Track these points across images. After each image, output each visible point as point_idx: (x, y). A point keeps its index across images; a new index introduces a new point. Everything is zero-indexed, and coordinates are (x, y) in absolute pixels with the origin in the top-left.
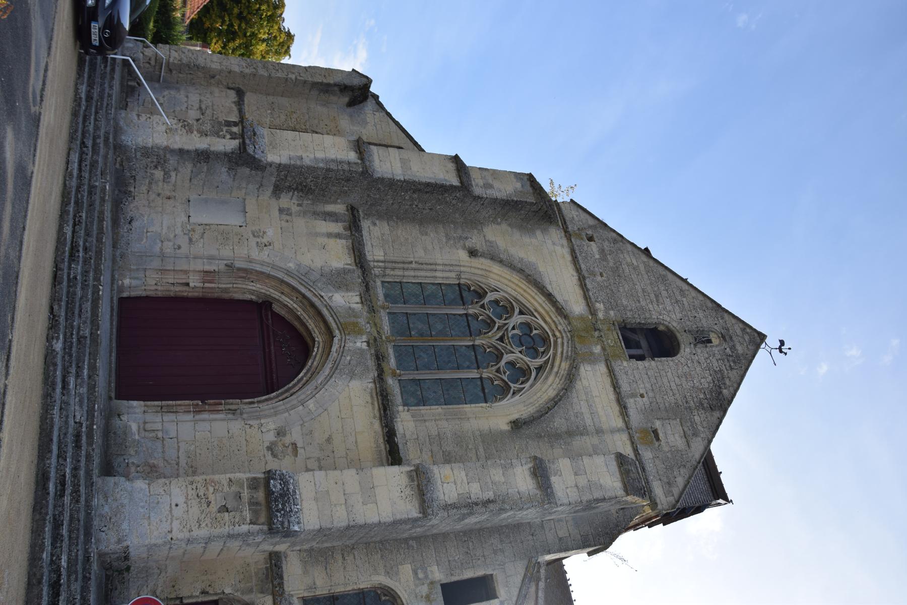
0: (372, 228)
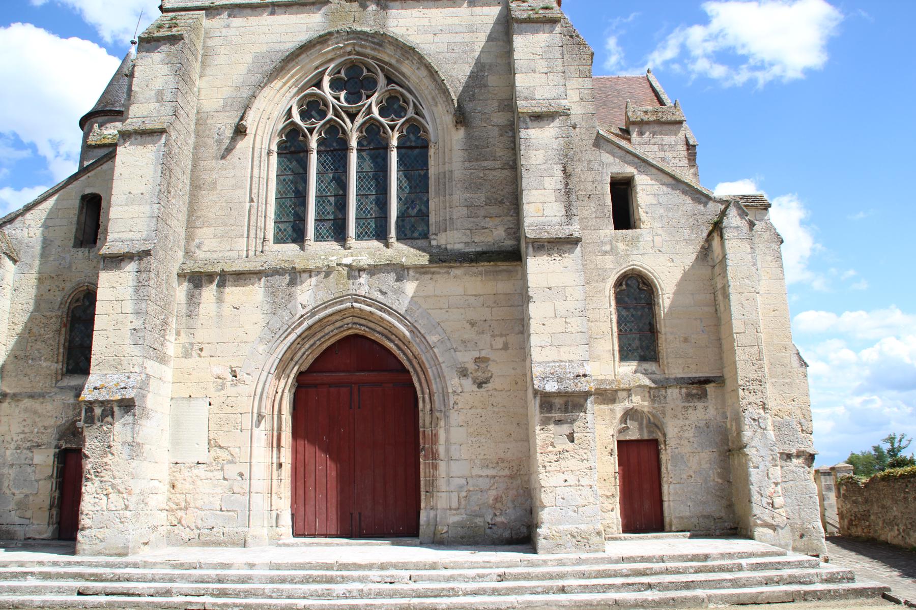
0: (205, 248)
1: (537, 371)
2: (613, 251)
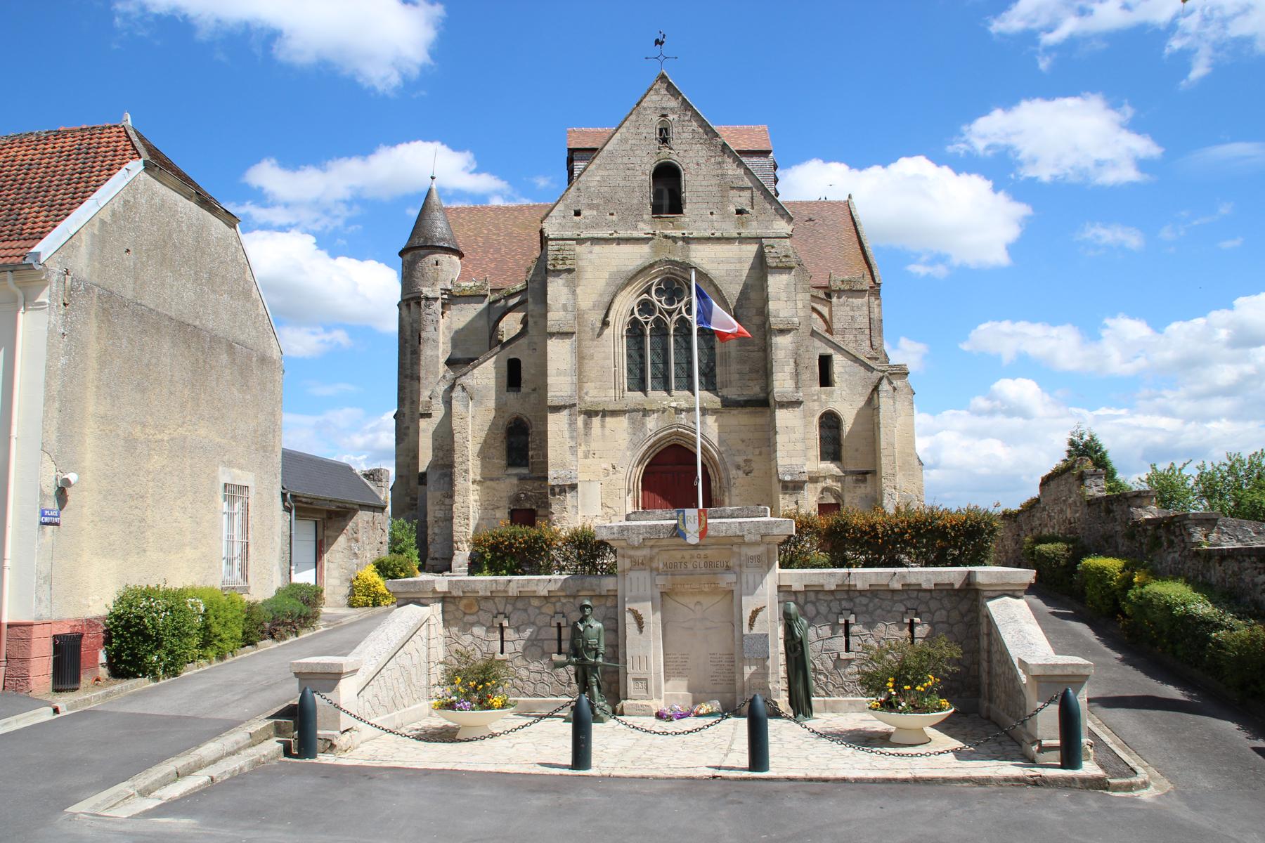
1: (780, 470)
2: (819, 400)
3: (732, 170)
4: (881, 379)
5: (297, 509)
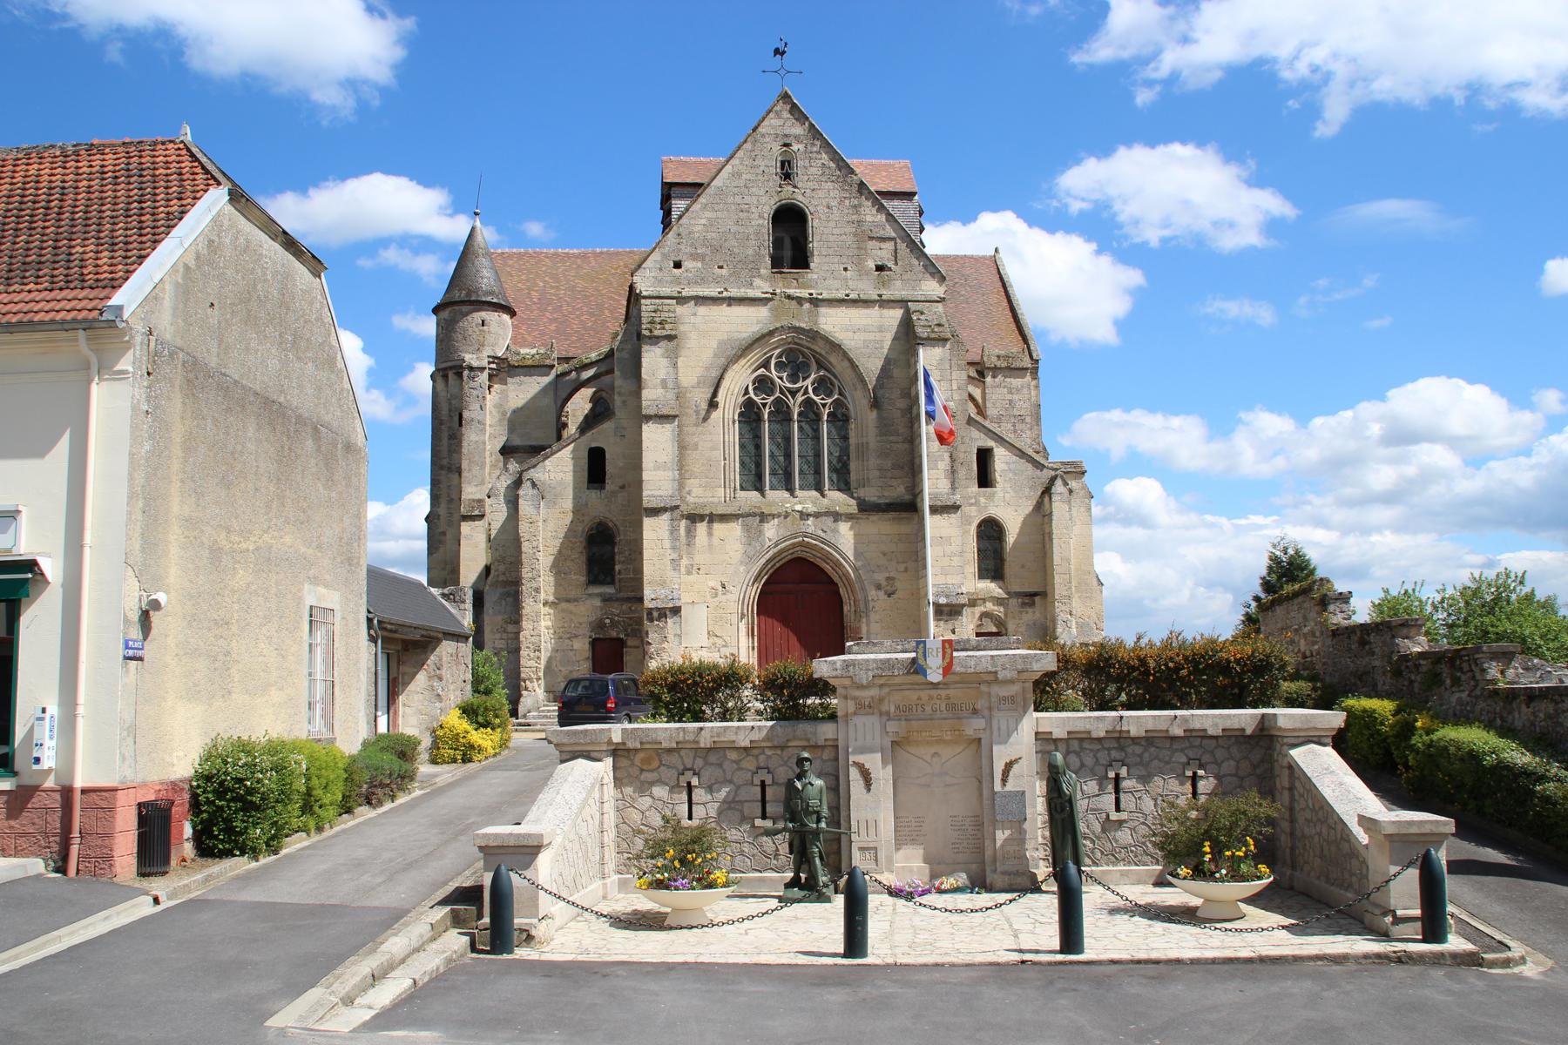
2: (976, 504)
3: (870, 215)
4: (1053, 480)
5: (385, 640)
